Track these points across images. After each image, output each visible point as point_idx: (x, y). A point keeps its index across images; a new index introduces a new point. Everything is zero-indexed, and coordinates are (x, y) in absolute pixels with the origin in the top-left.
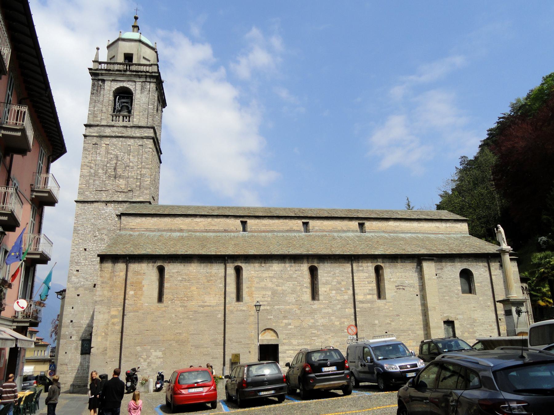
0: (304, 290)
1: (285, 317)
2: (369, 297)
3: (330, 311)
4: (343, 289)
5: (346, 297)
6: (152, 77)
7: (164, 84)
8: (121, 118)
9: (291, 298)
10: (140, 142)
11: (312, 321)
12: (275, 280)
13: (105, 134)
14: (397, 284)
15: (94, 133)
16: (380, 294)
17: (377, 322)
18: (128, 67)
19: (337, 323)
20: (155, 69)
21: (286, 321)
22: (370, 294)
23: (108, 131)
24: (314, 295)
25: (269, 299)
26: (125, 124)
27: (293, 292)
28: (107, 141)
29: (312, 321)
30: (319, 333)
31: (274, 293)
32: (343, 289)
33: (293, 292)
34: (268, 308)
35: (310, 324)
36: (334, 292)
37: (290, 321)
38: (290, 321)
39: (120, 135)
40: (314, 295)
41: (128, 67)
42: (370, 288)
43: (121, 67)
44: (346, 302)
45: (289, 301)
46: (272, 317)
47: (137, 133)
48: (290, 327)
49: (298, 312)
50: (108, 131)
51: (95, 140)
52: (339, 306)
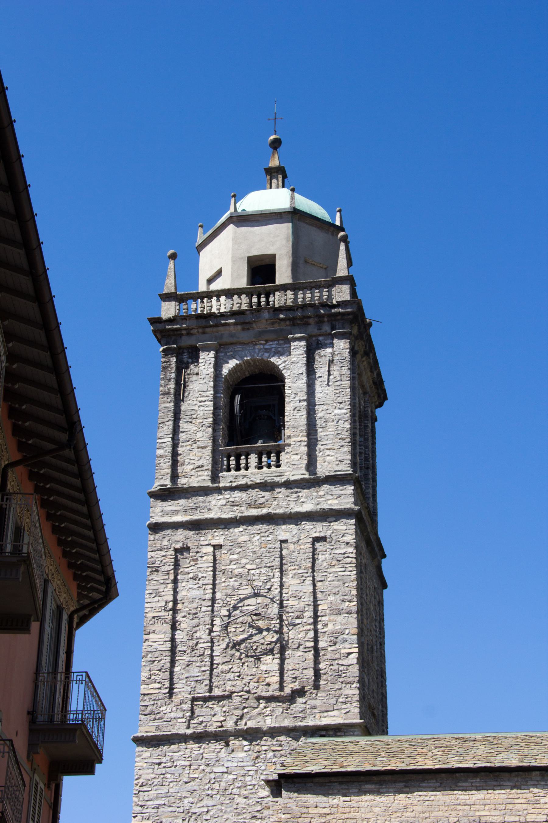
6: (335, 320)
7: (373, 331)
8: (253, 459)
13: (212, 515)
15: (176, 512)
18: (263, 299)
20: (342, 293)
23: (216, 507)
26: (267, 474)
28: (217, 537)
39: (254, 512)
41: (263, 299)
43: (243, 303)
47: (307, 500)
50: (216, 507)
51: (180, 535)
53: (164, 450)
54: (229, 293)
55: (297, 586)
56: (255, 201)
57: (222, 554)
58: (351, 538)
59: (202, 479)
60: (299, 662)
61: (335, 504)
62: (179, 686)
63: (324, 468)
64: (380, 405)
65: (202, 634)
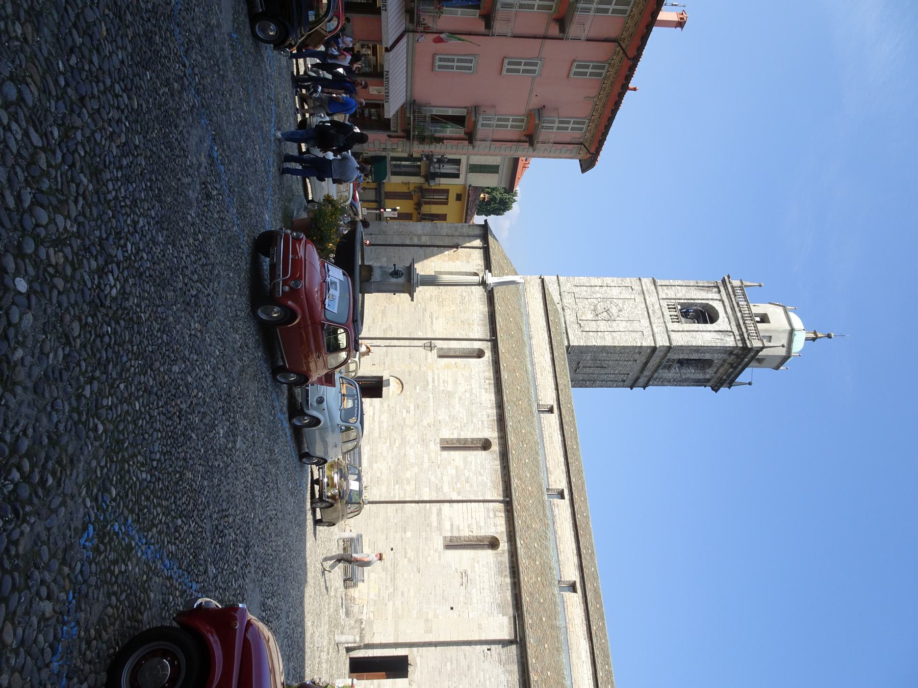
0: (456, 432)
1: (417, 407)
2: (447, 525)
3: (426, 465)
4: (459, 485)
5: (446, 489)
9: (443, 415)
10: (647, 332)
11: (412, 441)
12: (468, 395)
14: (469, 573)
16: (453, 544)
17: (409, 534)
19: (408, 475)
21: (412, 407)
22: (452, 526)
24: (449, 446)
25: (442, 388)
27: (453, 418)
28: (639, 299)
29: (412, 441)
30: (395, 449)
31: (450, 395)
32: (459, 485)
33: (453, 418)
34: (430, 387)
35: (408, 438)
36: (454, 472)
37: (412, 412)
38: (412, 412)
39: (650, 312)
40: (449, 446)
42: (461, 528)
44: (439, 489)
45: (439, 412)
46: (418, 390)
48: (405, 411)
49: (425, 423)
50: (652, 299)
52: (433, 479)
53: (672, 282)
54: (749, 308)
55: (622, 326)
56: (795, 318)
57: (632, 302)
58: (644, 344)
59: (662, 295)
60: (593, 326)
61: (658, 338)
62: (578, 289)
63: (673, 335)
64: (713, 389)
65: (599, 295)
